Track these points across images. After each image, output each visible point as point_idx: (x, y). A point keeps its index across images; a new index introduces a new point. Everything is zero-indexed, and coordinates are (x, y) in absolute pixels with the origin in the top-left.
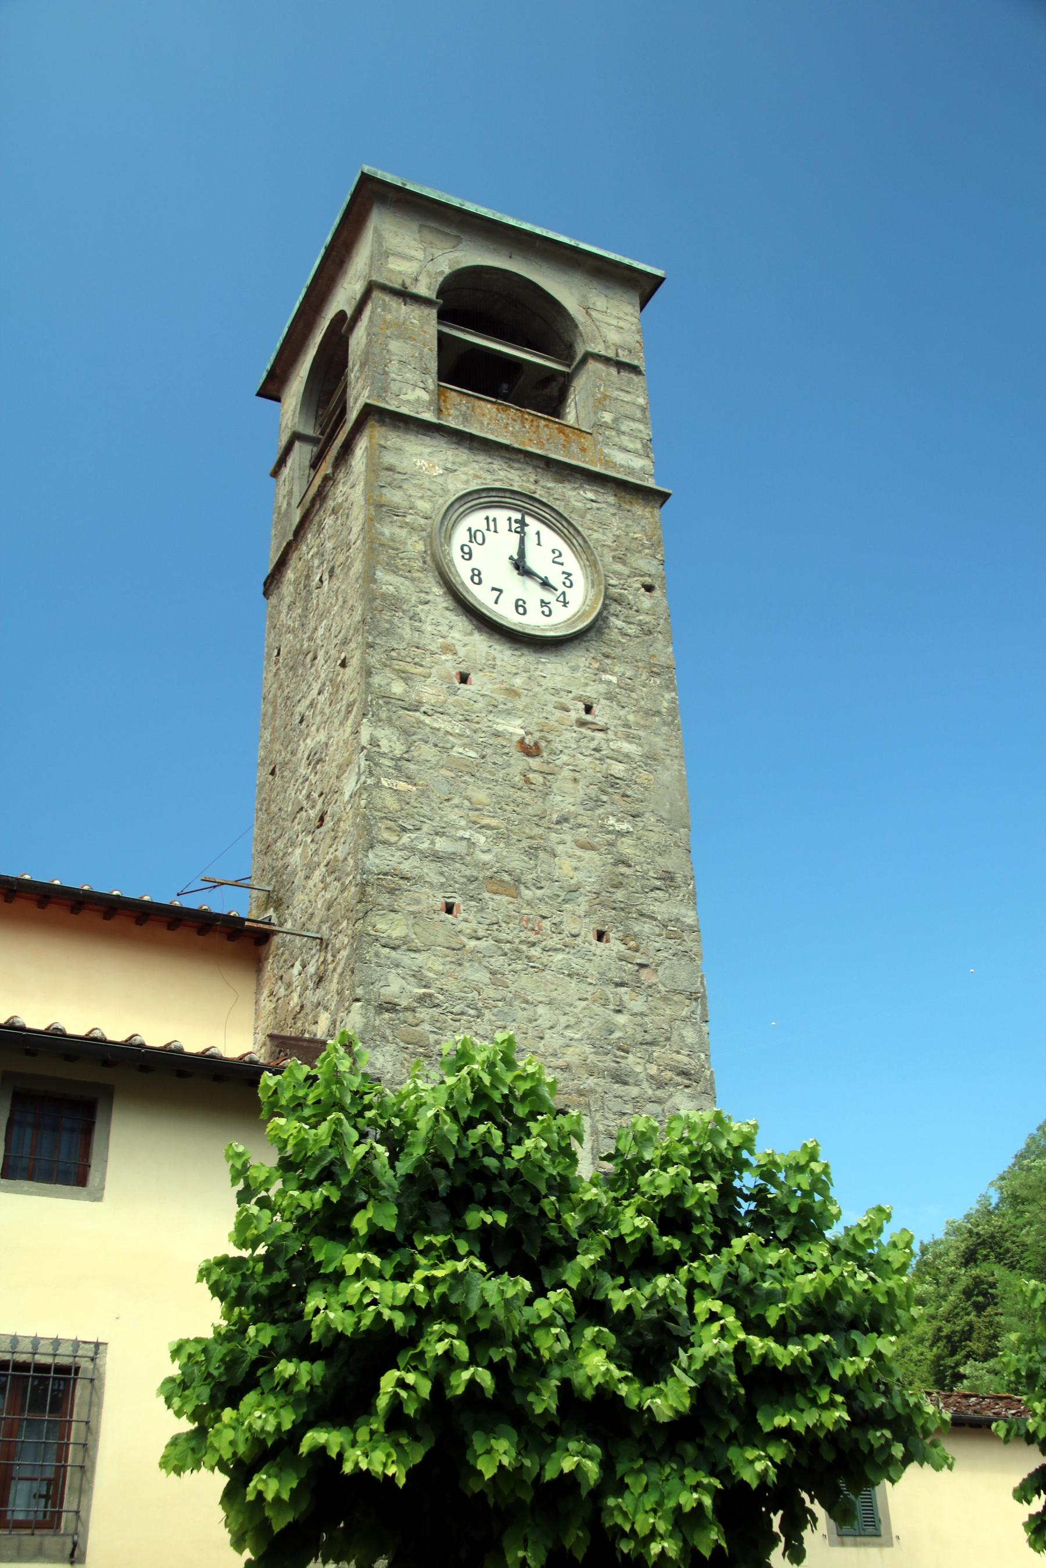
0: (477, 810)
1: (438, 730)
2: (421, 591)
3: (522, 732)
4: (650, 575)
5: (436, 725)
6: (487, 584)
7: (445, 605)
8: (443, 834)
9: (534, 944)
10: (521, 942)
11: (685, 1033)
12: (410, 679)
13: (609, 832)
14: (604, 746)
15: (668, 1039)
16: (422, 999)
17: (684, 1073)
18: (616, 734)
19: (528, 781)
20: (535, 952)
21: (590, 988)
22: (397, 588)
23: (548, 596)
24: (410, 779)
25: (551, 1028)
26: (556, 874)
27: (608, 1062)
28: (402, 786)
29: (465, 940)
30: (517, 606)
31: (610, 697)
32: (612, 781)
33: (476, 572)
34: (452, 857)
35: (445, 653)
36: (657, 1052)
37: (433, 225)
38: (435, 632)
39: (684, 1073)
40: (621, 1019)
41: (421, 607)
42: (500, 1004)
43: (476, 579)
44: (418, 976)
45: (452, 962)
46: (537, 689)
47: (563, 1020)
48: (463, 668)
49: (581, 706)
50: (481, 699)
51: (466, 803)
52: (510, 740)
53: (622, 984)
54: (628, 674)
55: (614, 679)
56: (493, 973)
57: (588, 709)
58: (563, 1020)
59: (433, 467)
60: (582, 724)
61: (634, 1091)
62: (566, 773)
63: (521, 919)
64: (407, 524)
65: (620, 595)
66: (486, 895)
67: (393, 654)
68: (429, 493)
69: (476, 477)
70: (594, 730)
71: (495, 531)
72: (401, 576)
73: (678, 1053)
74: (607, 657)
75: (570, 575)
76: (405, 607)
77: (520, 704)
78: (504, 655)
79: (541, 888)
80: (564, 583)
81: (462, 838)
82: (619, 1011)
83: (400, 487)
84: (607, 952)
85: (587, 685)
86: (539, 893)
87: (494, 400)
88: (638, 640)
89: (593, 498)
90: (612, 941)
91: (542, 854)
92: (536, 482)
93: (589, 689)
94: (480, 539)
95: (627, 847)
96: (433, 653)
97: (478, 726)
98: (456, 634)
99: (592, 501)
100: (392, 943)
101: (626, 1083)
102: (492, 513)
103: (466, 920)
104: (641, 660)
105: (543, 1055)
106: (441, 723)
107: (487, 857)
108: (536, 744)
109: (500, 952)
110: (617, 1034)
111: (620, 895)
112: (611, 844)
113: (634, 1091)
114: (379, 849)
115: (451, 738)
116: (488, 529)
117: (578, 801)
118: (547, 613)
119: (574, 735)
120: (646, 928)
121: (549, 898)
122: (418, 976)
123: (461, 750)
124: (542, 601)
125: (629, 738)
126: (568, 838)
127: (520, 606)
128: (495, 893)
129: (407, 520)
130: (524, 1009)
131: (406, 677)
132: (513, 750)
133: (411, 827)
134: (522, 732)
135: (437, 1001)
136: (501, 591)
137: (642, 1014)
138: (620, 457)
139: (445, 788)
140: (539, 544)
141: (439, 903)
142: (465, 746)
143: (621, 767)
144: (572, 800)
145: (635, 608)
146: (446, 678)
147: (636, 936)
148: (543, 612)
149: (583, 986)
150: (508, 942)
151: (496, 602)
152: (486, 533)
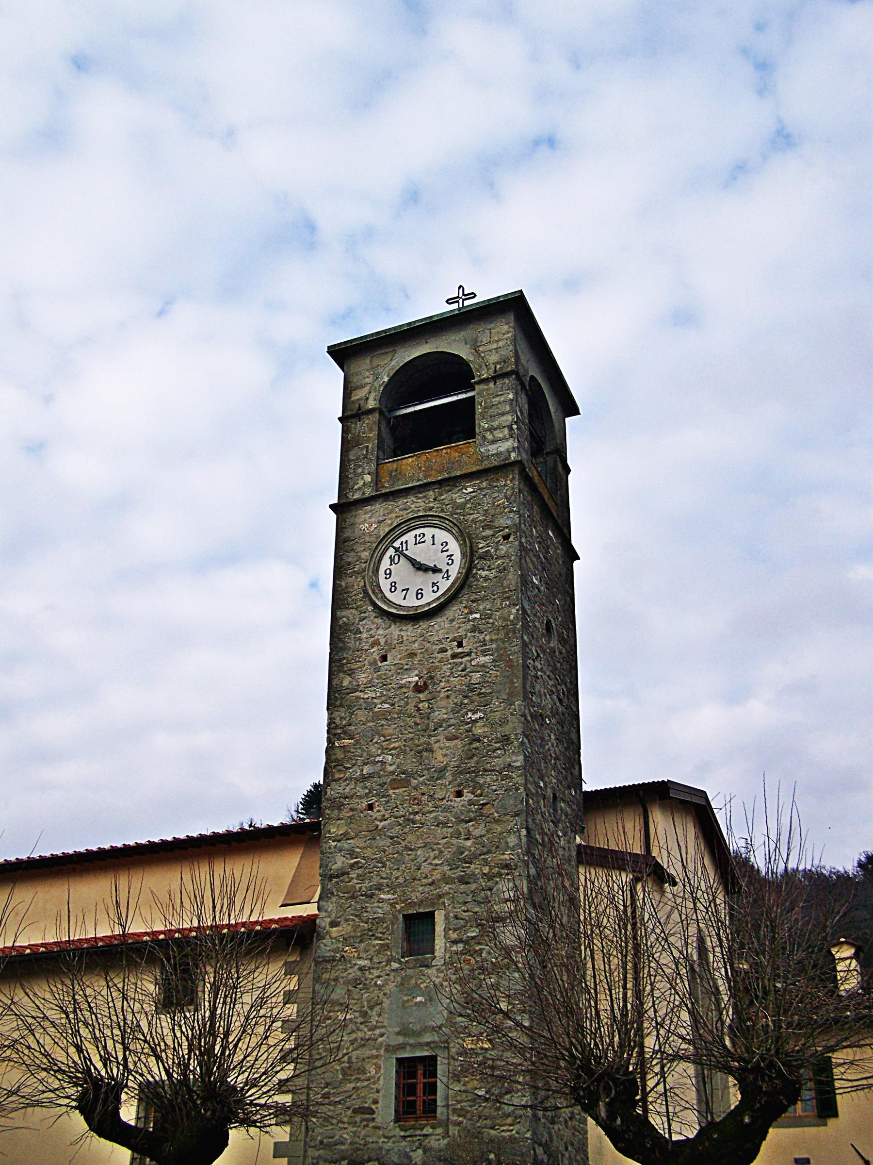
0: (387, 740)
1: (368, 698)
3: (417, 678)
4: (507, 527)
5: (366, 696)
6: (399, 588)
7: (374, 615)
8: (368, 763)
9: (417, 813)
10: (410, 814)
11: (509, 840)
12: (354, 673)
13: (468, 723)
14: (468, 665)
15: (497, 847)
16: (352, 866)
17: (507, 866)
18: (476, 653)
19: (419, 709)
20: (417, 817)
21: (450, 830)
22: (348, 618)
25: (425, 861)
26: (433, 762)
27: (458, 873)
29: (378, 823)
30: (417, 594)
32: (471, 688)
33: (393, 584)
34: (371, 776)
35: (373, 647)
36: (490, 857)
37: (380, 352)
38: (369, 636)
40: (468, 843)
42: (395, 856)
43: (393, 589)
44: (352, 854)
45: (370, 839)
46: (428, 645)
47: (432, 854)
48: (383, 652)
49: (456, 643)
50: (393, 667)
51: (382, 738)
52: (409, 687)
53: (470, 821)
54: (488, 607)
55: (478, 616)
56: (392, 838)
58: (432, 854)
60: (454, 656)
61: (473, 886)
62: (442, 695)
63: (410, 800)
64: (355, 572)
65: (486, 552)
66: (391, 792)
67: (345, 661)
68: (369, 544)
69: (397, 517)
70: (462, 658)
72: (351, 608)
73: (504, 854)
74: (473, 601)
75: (452, 555)
76: (352, 628)
77: (416, 660)
78: (409, 632)
79: (424, 776)
80: (448, 564)
81: (378, 761)
82: (468, 839)
83: (353, 550)
84: (462, 803)
85: (459, 627)
86: (421, 779)
87: (412, 454)
89: (472, 490)
90: (465, 794)
91: (424, 754)
92: (435, 499)
93: (460, 630)
94: (396, 561)
95: (478, 730)
96: (367, 650)
97: (390, 686)
98: (381, 632)
99: (471, 492)
100: (338, 838)
101: (467, 883)
103: (379, 811)
104: (497, 593)
105: (419, 880)
107: (392, 768)
108: (425, 683)
109: (397, 824)
110: (467, 853)
112: (470, 730)
113: (473, 886)
115: (375, 701)
117: (449, 710)
119: (449, 666)
121: (428, 780)
122: (352, 854)
123: (380, 706)
124: (433, 583)
125: (484, 653)
126: (441, 737)
128: (396, 788)
130: (409, 855)
132: (410, 694)
133: (350, 766)
134: (417, 678)
135: (361, 865)
136: (408, 589)
137: (481, 836)
138: (493, 449)
139: (370, 735)
140: (434, 544)
142: (381, 703)
143: (478, 675)
144: (444, 711)
147: (481, 786)
148: (433, 591)
149: (445, 830)
150: (402, 816)
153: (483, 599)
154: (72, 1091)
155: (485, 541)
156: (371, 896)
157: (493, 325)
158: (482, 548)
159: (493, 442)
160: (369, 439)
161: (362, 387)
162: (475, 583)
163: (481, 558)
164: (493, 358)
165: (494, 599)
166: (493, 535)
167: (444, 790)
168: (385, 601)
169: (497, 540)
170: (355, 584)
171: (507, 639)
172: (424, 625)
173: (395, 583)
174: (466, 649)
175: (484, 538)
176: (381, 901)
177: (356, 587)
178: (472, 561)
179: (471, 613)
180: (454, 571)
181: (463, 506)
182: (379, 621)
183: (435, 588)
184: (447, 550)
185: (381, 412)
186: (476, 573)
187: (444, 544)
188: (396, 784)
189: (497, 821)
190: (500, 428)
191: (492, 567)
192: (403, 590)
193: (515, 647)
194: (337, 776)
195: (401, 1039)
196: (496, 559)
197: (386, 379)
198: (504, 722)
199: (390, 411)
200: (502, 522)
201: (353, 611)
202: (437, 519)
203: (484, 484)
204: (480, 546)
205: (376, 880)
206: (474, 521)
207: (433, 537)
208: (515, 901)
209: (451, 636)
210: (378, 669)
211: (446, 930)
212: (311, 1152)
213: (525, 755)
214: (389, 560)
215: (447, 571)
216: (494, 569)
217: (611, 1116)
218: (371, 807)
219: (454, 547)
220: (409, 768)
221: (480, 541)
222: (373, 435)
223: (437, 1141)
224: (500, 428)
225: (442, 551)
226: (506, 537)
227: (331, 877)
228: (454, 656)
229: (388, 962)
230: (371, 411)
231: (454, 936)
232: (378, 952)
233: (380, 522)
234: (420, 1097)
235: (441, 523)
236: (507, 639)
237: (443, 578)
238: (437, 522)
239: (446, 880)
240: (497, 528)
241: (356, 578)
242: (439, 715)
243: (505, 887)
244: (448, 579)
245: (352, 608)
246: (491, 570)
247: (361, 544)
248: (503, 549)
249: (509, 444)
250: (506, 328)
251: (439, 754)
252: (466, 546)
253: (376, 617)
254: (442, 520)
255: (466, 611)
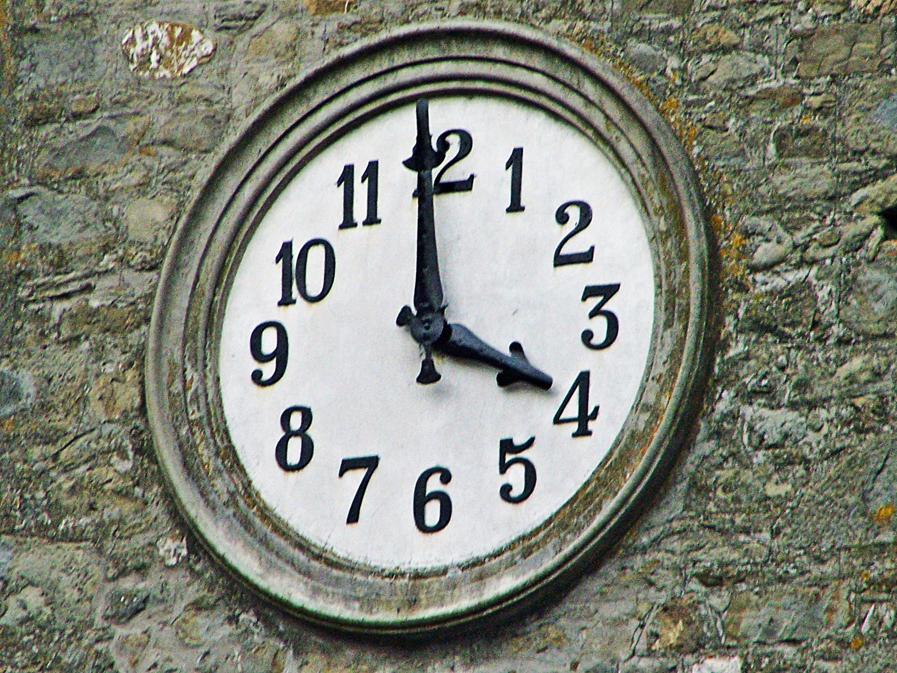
2: (123, 573)
7: (195, 591)
30: (421, 499)
33: (296, 421)
41: (120, 631)
43: (294, 454)
54: (787, 623)
59: (186, 36)
65: (790, 292)
71: (372, 219)
72: (67, 537)
75: (609, 291)
80: (587, 336)
83: (79, 174)
88: (832, 468)
94: (314, 284)
104: (834, 551)
116: (348, 223)
118: (518, 490)
124: (507, 446)
129: (94, 303)
136: (371, 464)
140: (516, 206)
145: (837, 330)
151: (353, 517)
152: (342, 242)
155: (791, 227)
158: (768, 267)
162: (726, 474)
165: (821, 583)
166: (833, 198)
168: (247, 525)
169: (850, 230)
170: (93, 393)
173: (307, 415)
177: (96, 409)
183: (516, 476)
184: (587, 257)
186: (733, 416)
187: (574, 214)
191: (819, 390)
192: (348, 465)
196: (842, 342)
201: (80, 555)
202: (537, 61)
204: (764, 252)
207: (516, 159)
214: (277, 270)
215: (583, 380)
216: (824, 402)
221: (764, 223)
225: (561, 260)
235: (556, 90)
237: (557, 421)
238: (537, 80)
240: (858, 154)
241: (99, 353)
244: (583, 432)
245: (74, 537)
246: (812, 405)
247: (126, 145)
252: (684, 255)
253: (198, 606)
254: (565, 74)
255: (672, 636)
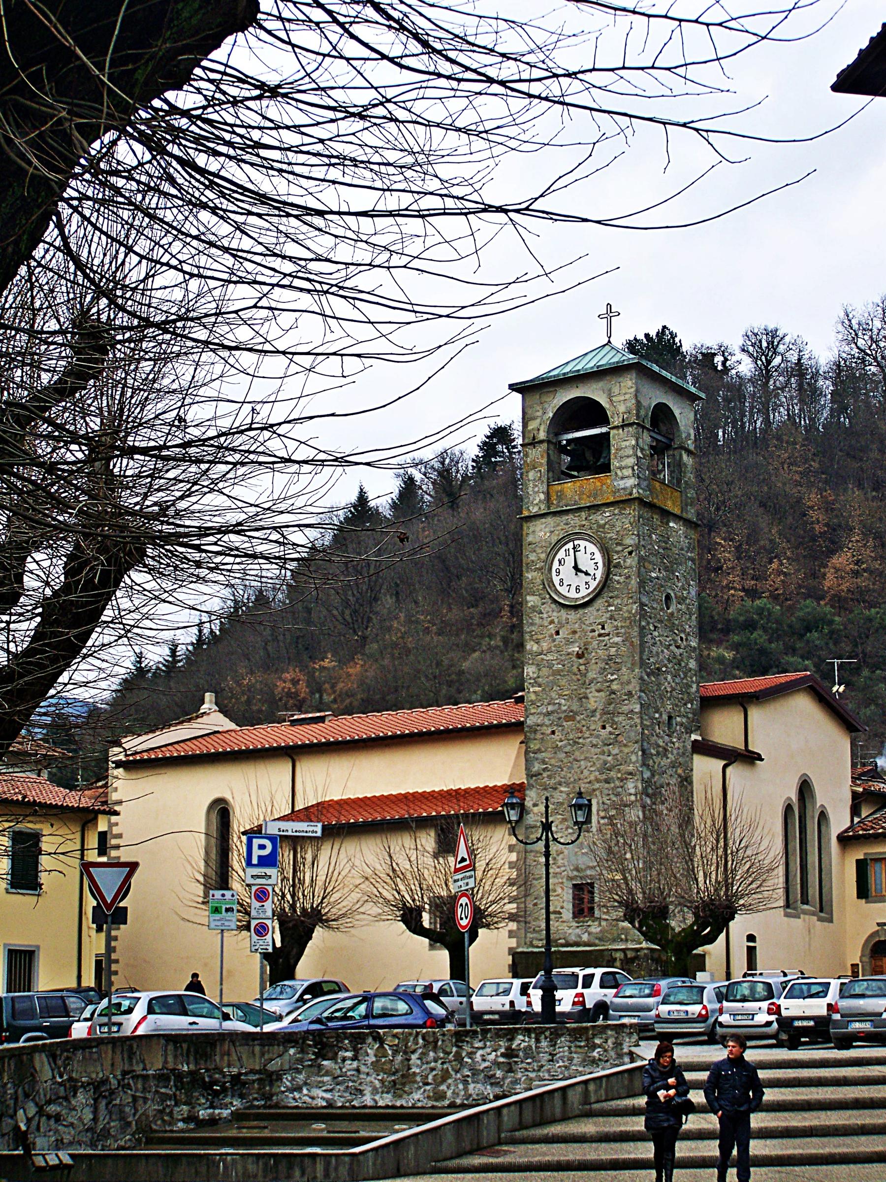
6: (565, 584)
16: (544, 770)
17: (631, 774)
20: (581, 741)
23: (588, 579)
24: (540, 686)
27: (604, 776)
28: (537, 689)
31: (611, 618)
34: (553, 712)
36: (622, 767)
39: (631, 774)
40: (610, 758)
57: (603, 628)
60: (600, 635)
77: (577, 636)
78: (573, 616)
95: (615, 687)
102: (566, 547)
106: (550, 657)
111: (611, 708)
114: (531, 717)
120: (621, 718)
125: (618, 635)
127: (578, 589)
131: (537, 642)
132: (574, 659)
138: (622, 484)
141: (549, 731)
146: (551, 636)
153: (617, 597)
154: (398, 913)
156: (555, 789)
157: (621, 379)
159: (622, 478)
160: (541, 464)
161: (534, 419)
163: (615, 567)
164: (622, 408)
167: (595, 723)
171: (630, 626)
172: (581, 611)
174: (606, 631)
175: (617, 552)
176: (561, 792)
178: (609, 569)
179: (609, 605)
180: (599, 574)
181: (603, 526)
182: (553, 606)
185: (549, 442)
188: (568, 718)
189: (625, 746)
190: (626, 467)
193: (635, 632)
194: (533, 711)
195: (575, 873)
197: (551, 415)
198: (629, 682)
199: (557, 434)
200: (628, 541)
203: (616, 511)
205: (558, 779)
206: (611, 539)
208: (636, 795)
209: (598, 621)
210: (554, 641)
211: (598, 811)
212: (530, 935)
213: (641, 704)
217: (641, 926)
218: (553, 733)
219: (598, 557)
220: (574, 708)
222: (544, 461)
223: (595, 929)
224: (626, 467)
226: (630, 553)
227: (532, 776)
228: (600, 635)
229: (567, 828)
230: (541, 442)
231: (602, 814)
232: (561, 822)
233: (552, 532)
234: (586, 905)
236: (630, 626)
239: (598, 781)
242: (591, 675)
243: (631, 786)
248: (629, 561)
249: (632, 482)
250: (630, 383)
251: (592, 700)
